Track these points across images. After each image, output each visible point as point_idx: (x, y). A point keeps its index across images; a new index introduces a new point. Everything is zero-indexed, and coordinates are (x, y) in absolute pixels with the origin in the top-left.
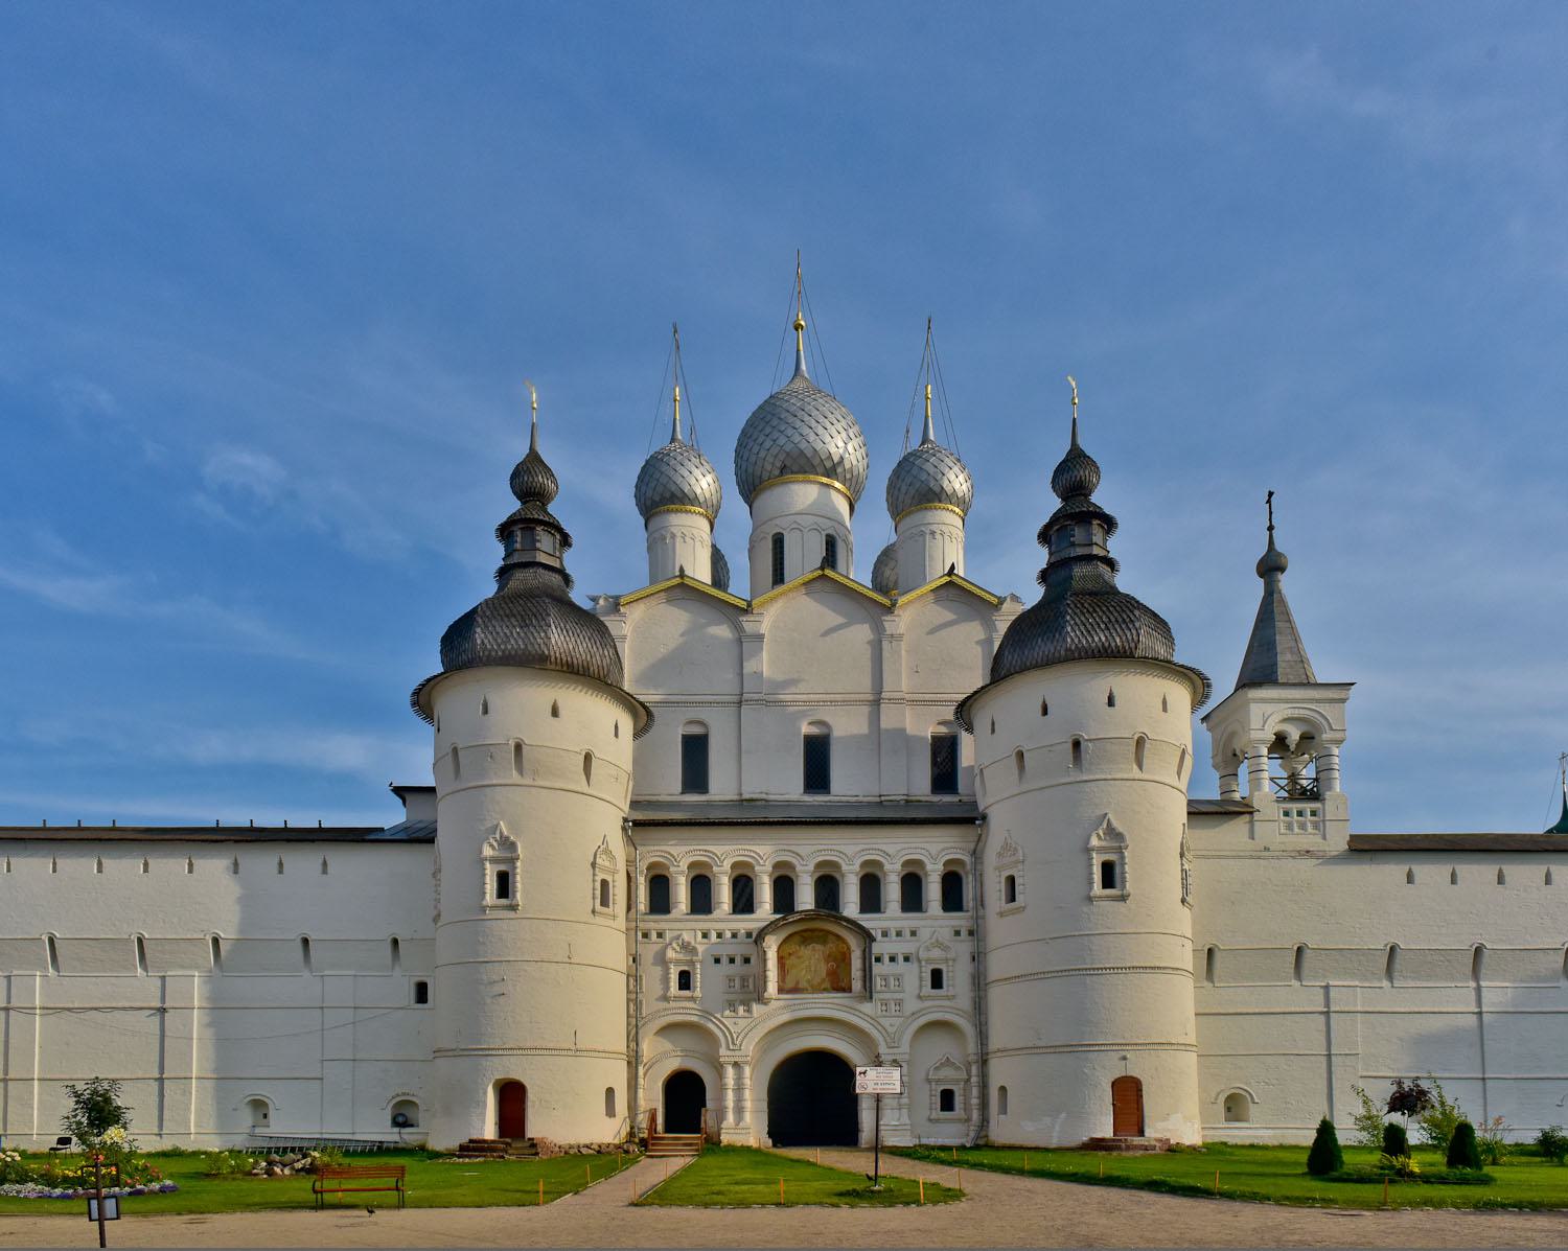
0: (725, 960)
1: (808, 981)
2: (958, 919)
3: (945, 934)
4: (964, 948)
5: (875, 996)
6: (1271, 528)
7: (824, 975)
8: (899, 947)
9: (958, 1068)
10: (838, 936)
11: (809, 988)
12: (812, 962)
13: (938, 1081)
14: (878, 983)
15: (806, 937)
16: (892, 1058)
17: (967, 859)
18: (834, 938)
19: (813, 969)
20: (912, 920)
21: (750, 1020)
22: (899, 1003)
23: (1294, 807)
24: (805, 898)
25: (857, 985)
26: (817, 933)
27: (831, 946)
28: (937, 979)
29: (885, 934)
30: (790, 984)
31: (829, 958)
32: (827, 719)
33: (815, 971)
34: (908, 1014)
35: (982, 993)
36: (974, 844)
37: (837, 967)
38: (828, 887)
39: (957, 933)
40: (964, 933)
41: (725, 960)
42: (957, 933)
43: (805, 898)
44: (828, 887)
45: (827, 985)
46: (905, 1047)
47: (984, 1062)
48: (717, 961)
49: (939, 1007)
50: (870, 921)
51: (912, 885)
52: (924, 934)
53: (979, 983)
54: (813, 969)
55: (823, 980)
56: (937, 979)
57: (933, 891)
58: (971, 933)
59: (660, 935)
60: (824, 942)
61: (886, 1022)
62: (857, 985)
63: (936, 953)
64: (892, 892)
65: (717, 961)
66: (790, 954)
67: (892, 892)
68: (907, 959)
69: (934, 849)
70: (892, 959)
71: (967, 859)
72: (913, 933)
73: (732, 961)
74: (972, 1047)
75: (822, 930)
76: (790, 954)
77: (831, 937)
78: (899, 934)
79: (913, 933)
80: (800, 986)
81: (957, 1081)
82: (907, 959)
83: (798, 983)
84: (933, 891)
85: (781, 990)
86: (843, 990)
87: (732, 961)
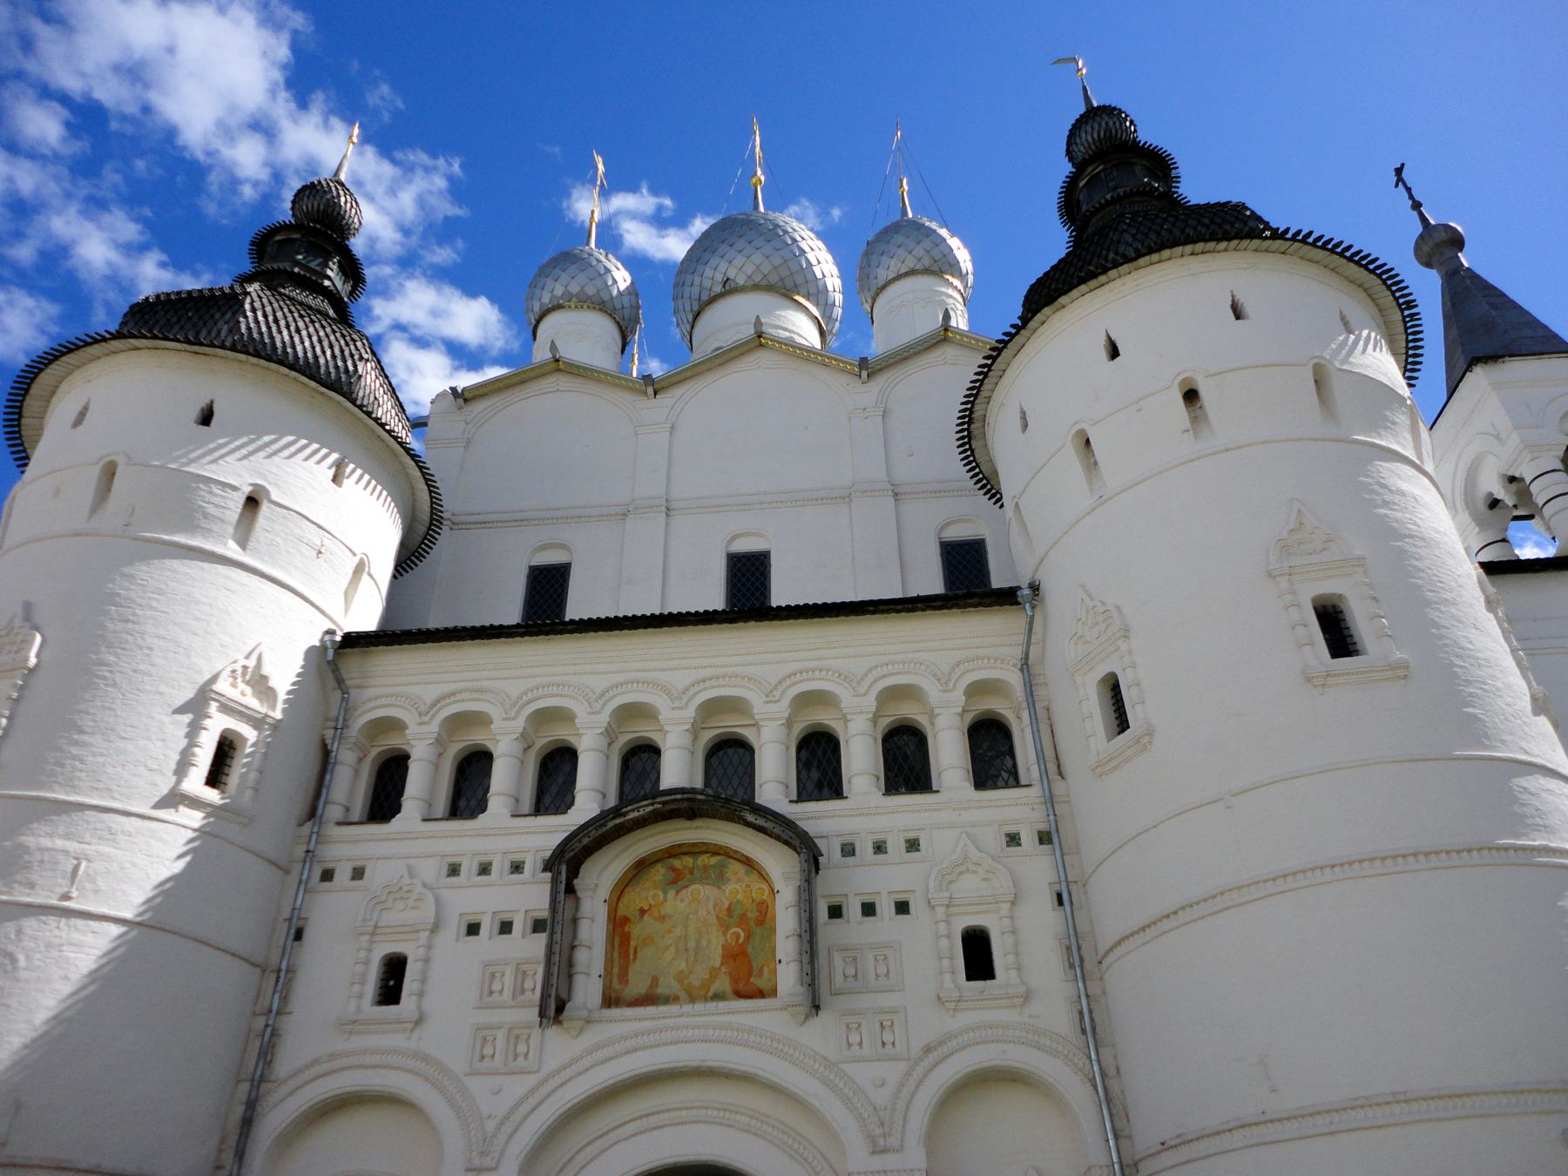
1: (680, 977)
6: (1417, 206)
7: (717, 961)
10: (748, 862)
11: (683, 995)
14: (836, 969)
19: (692, 945)
21: (532, 1080)
25: (788, 977)
26: (704, 860)
28: (978, 955)
30: (637, 984)
33: (697, 950)
34: (916, 1050)
35: (1094, 988)
37: (747, 938)
39: (1013, 839)
40: (1028, 839)
45: (723, 984)
49: (985, 1026)
53: (1080, 958)
54: (692, 945)
55: (714, 974)
56: (978, 955)
61: (864, 1074)
64: (861, 759)
65: (473, 929)
66: (643, 912)
67: (861, 759)
69: (944, 666)
72: (913, 845)
73: (506, 928)
76: (643, 912)
77: (734, 867)
78: (879, 848)
79: (913, 845)
80: (660, 991)
82: (902, 908)
83: (655, 981)
84: (949, 753)
85: (611, 1000)
86: (760, 994)
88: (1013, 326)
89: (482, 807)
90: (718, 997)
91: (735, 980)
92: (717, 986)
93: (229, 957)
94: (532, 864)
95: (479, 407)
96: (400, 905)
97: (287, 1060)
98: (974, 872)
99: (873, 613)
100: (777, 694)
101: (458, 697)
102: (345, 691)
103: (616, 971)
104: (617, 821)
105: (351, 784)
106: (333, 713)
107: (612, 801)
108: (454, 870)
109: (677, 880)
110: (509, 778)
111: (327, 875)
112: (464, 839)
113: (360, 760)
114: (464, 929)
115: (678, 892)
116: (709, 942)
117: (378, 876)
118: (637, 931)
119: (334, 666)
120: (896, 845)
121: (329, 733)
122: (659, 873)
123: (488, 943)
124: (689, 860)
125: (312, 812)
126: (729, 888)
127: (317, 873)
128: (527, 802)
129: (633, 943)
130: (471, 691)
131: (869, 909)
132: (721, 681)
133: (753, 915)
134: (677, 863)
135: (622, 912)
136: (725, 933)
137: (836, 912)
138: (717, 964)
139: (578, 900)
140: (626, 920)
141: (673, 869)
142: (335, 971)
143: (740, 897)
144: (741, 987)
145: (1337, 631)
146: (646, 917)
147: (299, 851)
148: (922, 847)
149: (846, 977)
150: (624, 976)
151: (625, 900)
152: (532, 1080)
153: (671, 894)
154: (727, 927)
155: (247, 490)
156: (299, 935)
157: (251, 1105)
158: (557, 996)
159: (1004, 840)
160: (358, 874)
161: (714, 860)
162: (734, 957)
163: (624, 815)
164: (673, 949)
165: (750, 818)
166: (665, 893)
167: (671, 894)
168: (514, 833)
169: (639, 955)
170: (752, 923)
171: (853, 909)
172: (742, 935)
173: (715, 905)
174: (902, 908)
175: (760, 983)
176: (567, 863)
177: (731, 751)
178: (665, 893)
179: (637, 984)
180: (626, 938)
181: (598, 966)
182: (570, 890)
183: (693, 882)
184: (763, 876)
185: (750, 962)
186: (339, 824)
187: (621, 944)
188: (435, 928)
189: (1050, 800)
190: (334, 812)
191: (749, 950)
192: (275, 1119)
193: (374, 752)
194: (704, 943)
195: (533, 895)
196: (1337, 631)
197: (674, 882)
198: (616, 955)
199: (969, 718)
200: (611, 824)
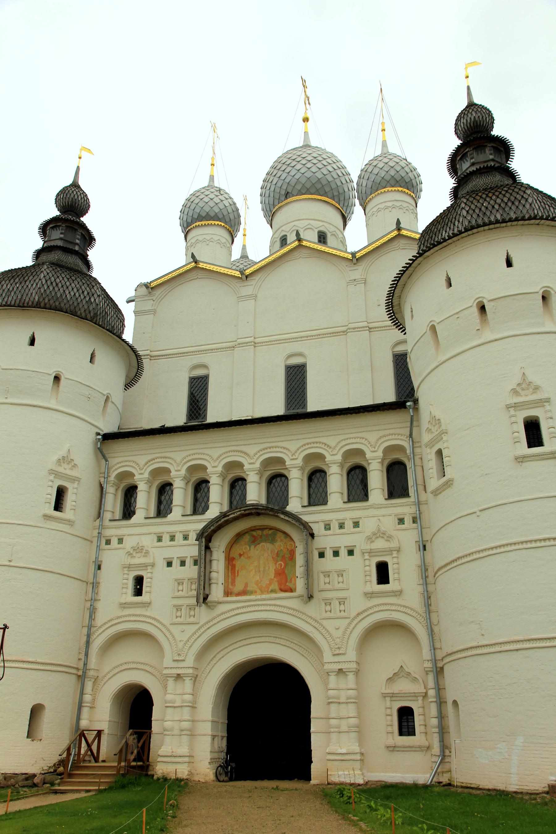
0: (176, 563)
1: (257, 583)
2: (403, 507)
3: (389, 524)
4: (408, 537)
5: (316, 594)
8: (342, 541)
9: (415, 680)
10: (284, 533)
11: (258, 591)
12: (261, 562)
13: (393, 696)
14: (321, 582)
15: (255, 536)
16: (337, 667)
17: (406, 444)
18: (283, 536)
19: (262, 569)
20: (356, 510)
21: (196, 627)
22: (342, 601)
24: (255, 494)
26: (266, 532)
27: (280, 544)
28: (383, 573)
29: (328, 527)
30: (239, 587)
31: (277, 556)
32: (306, 352)
35: (431, 588)
36: (409, 429)
37: (285, 566)
38: (276, 481)
39: (401, 521)
40: (408, 520)
41: (176, 563)
42: (401, 521)
43: (255, 494)
44: (276, 481)
45: (275, 586)
46: (352, 654)
47: (439, 672)
48: (169, 564)
50: (314, 517)
51: (357, 477)
52: (369, 525)
54: (262, 569)
55: (271, 581)
56: (383, 573)
57: (377, 480)
58: (414, 521)
59: (120, 541)
60: (273, 540)
62: (300, 585)
63: (380, 544)
64: (336, 483)
67: (336, 483)
68: (351, 553)
70: (336, 554)
71: (406, 444)
72: (356, 524)
73: (183, 563)
74: (426, 653)
75: (271, 529)
76: (240, 555)
77: (279, 534)
78: (341, 526)
79: (356, 524)
80: (248, 589)
81: (415, 696)
83: (246, 585)
84: (377, 480)
85: (227, 593)
87: (183, 563)
88: (410, 260)
89: (169, 511)
90: (273, 591)
91: (280, 584)
92: (272, 587)
93: (73, 579)
94: (193, 536)
95: (158, 292)
96: (139, 555)
97: (100, 619)
98: (383, 537)
99: (340, 415)
100: (297, 455)
101: (156, 461)
102: (106, 460)
103: (230, 580)
104: (226, 519)
105: (114, 503)
106: (103, 471)
107: (226, 508)
108: (160, 539)
109: (255, 541)
110: (181, 497)
111: (108, 542)
112: (163, 526)
113: (117, 490)
114: (165, 564)
115: (255, 546)
116: (269, 568)
117: (129, 543)
118: (238, 563)
119: (100, 450)
120: (349, 524)
121: (102, 480)
122: (247, 538)
123: (177, 570)
124: (259, 532)
125: (99, 516)
126: (277, 544)
127: (103, 541)
128: (189, 510)
129: (237, 569)
130: (161, 458)
131: (336, 554)
132: (272, 450)
133: (288, 556)
134: (254, 533)
135: (231, 556)
136: (276, 564)
137: (322, 555)
138: (273, 577)
139: (211, 552)
140: (233, 559)
141: (253, 536)
142: (115, 586)
143: (282, 548)
144: (282, 587)
145: (533, 433)
146: (242, 557)
147: (95, 533)
148: (360, 525)
149: (325, 583)
150: (233, 583)
151: (233, 550)
152: (197, 627)
153: (253, 547)
154: (277, 561)
155: (54, 375)
156: (99, 568)
157: (89, 636)
158: (204, 593)
159: (397, 521)
160: (120, 541)
161: (270, 532)
162: (280, 574)
163: (228, 516)
164: (254, 571)
165: (282, 516)
166: (250, 547)
167: (253, 547)
168: (184, 523)
169: (240, 574)
170: (287, 559)
171: (329, 553)
172: (283, 564)
173: (272, 551)
174: (351, 553)
175: (290, 585)
176: (207, 537)
177: (279, 479)
178: (250, 547)
179: (239, 587)
180: (234, 567)
181: (221, 579)
182: (207, 548)
183: (262, 541)
184: (292, 539)
185: (286, 576)
186: (110, 520)
187: (232, 569)
188: (153, 565)
189: (419, 504)
190: (108, 516)
191: (286, 571)
192: (98, 642)
193: (122, 485)
194: (267, 568)
195: (192, 550)
196: (533, 433)
197: (253, 542)
198: (230, 574)
199: (386, 463)
200: (223, 520)
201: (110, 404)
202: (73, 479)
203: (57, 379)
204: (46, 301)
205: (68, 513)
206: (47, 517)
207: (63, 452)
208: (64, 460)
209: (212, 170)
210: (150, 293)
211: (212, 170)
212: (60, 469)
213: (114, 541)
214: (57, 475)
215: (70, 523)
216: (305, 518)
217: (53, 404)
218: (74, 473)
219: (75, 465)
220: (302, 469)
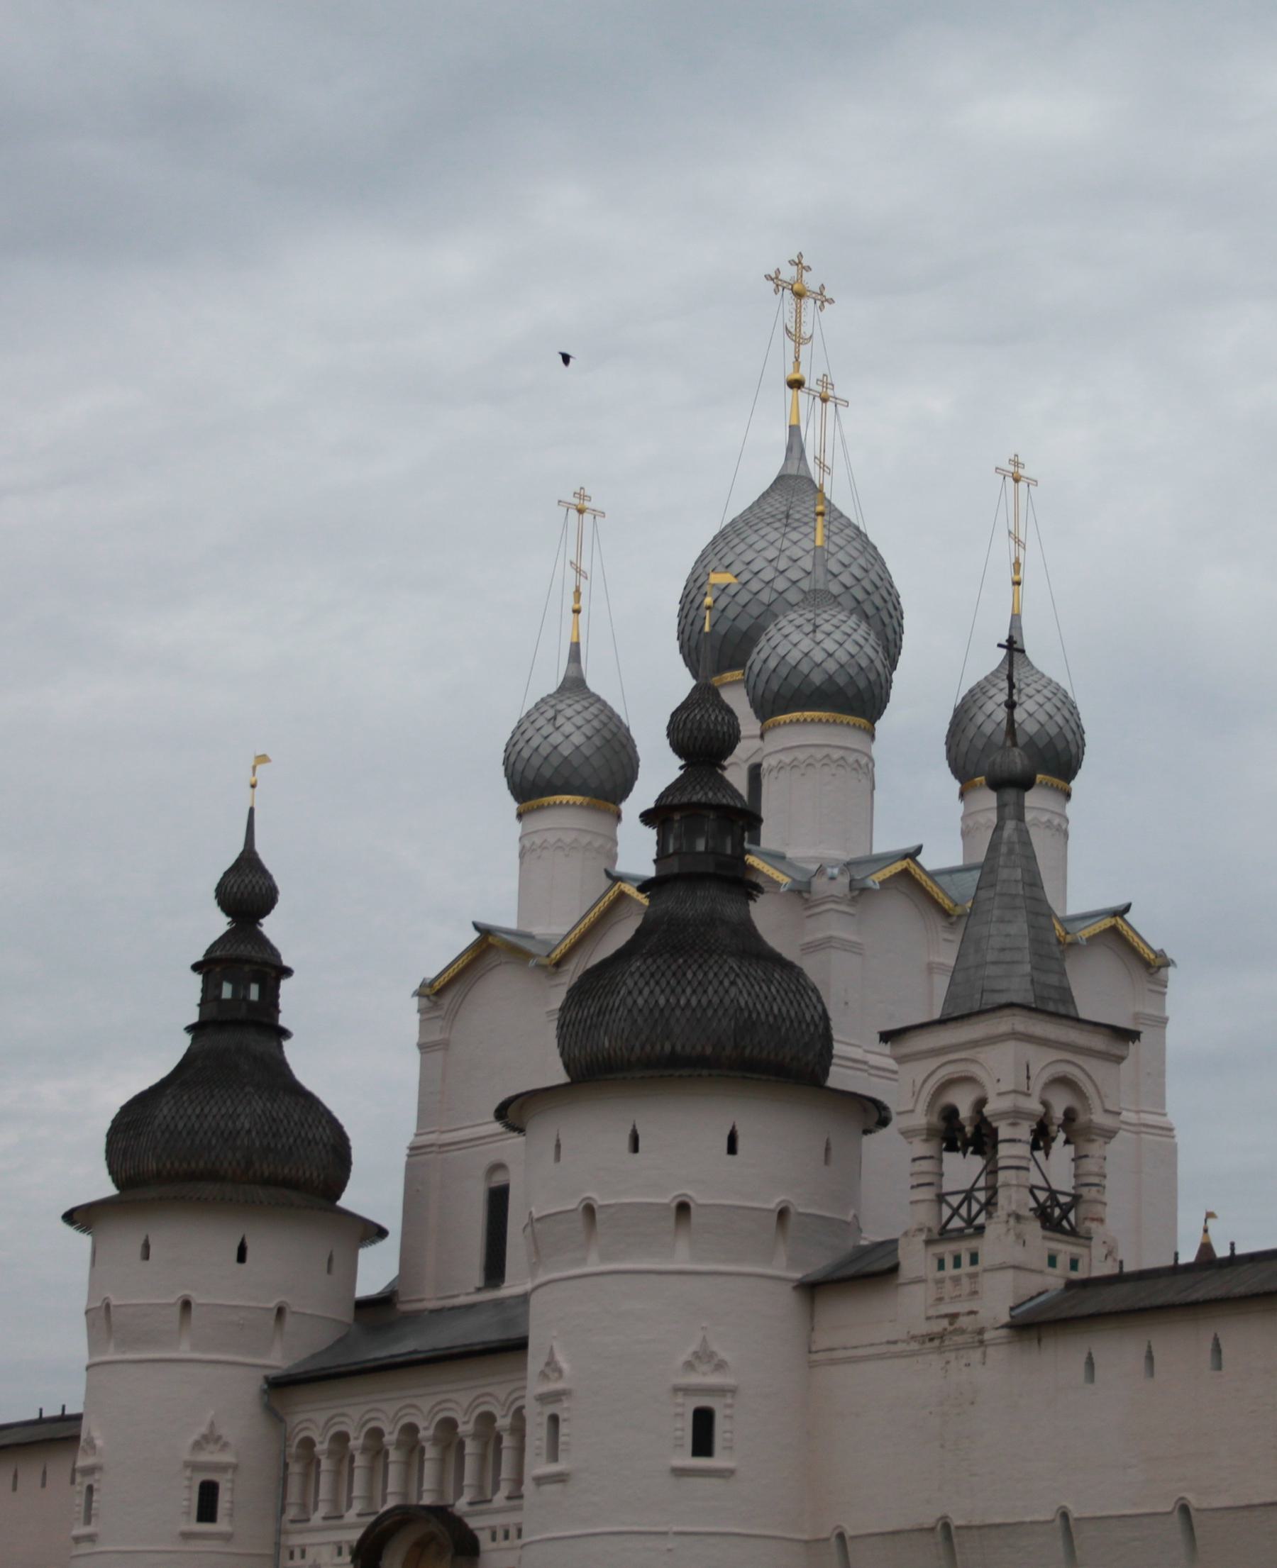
23: (947, 1250)
95: (446, 1000)
201: (289, 1318)
202: (223, 1468)
203: (186, 1305)
204: (168, 1165)
205: (222, 1525)
206: (187, 1536)
207: (203, 1430)
208: (210, 1438)
209: (576, 625)
210: (435, 1004)
211: (576, 625)
212: (204, 1457)
213: (297, 1554)
214: (195, 1467)
215: (227, 1537)
216: (472, 1523)
217: (184, 1351)
218: (227, 1458)
219: (226, 1445)
220: (475, 1436)
